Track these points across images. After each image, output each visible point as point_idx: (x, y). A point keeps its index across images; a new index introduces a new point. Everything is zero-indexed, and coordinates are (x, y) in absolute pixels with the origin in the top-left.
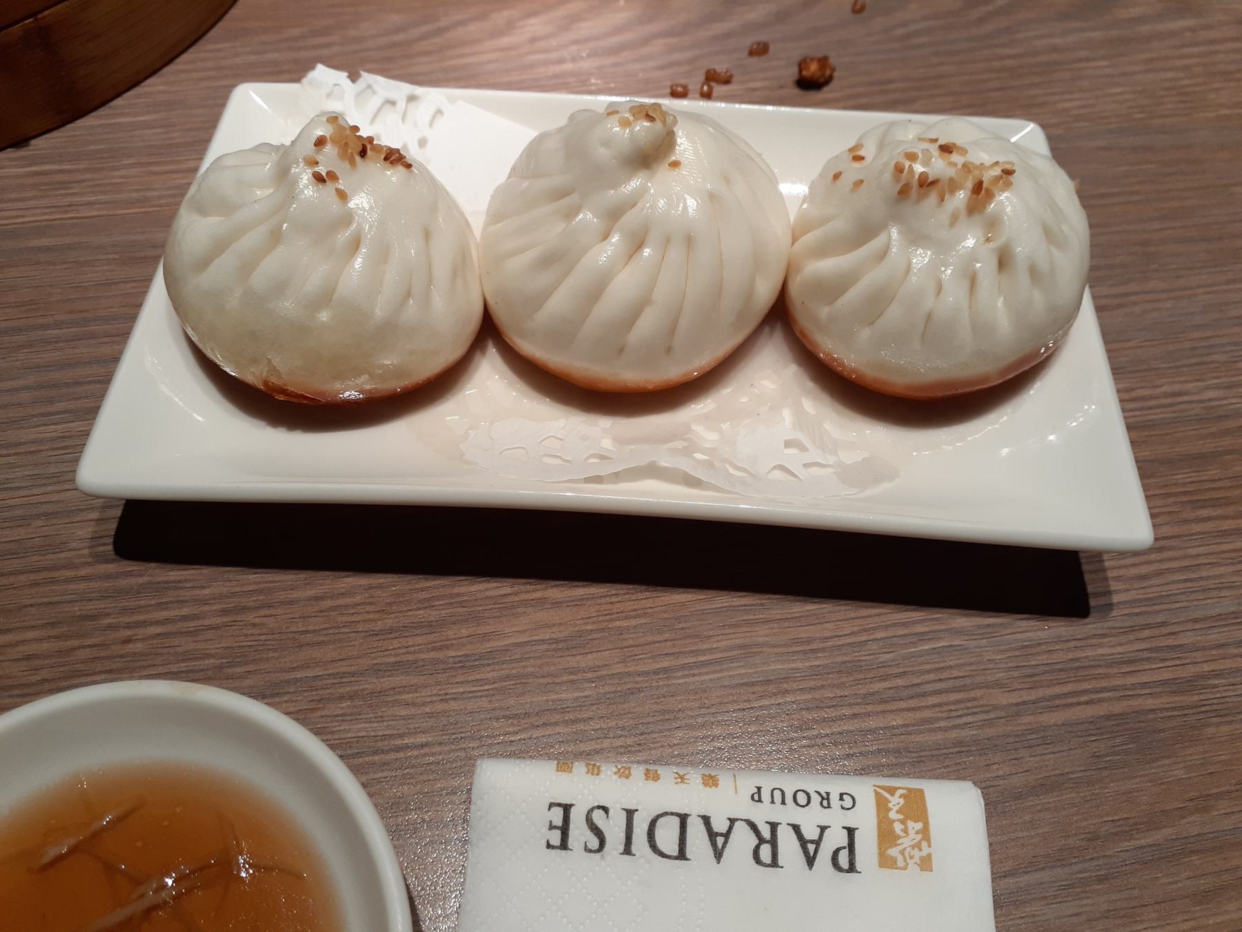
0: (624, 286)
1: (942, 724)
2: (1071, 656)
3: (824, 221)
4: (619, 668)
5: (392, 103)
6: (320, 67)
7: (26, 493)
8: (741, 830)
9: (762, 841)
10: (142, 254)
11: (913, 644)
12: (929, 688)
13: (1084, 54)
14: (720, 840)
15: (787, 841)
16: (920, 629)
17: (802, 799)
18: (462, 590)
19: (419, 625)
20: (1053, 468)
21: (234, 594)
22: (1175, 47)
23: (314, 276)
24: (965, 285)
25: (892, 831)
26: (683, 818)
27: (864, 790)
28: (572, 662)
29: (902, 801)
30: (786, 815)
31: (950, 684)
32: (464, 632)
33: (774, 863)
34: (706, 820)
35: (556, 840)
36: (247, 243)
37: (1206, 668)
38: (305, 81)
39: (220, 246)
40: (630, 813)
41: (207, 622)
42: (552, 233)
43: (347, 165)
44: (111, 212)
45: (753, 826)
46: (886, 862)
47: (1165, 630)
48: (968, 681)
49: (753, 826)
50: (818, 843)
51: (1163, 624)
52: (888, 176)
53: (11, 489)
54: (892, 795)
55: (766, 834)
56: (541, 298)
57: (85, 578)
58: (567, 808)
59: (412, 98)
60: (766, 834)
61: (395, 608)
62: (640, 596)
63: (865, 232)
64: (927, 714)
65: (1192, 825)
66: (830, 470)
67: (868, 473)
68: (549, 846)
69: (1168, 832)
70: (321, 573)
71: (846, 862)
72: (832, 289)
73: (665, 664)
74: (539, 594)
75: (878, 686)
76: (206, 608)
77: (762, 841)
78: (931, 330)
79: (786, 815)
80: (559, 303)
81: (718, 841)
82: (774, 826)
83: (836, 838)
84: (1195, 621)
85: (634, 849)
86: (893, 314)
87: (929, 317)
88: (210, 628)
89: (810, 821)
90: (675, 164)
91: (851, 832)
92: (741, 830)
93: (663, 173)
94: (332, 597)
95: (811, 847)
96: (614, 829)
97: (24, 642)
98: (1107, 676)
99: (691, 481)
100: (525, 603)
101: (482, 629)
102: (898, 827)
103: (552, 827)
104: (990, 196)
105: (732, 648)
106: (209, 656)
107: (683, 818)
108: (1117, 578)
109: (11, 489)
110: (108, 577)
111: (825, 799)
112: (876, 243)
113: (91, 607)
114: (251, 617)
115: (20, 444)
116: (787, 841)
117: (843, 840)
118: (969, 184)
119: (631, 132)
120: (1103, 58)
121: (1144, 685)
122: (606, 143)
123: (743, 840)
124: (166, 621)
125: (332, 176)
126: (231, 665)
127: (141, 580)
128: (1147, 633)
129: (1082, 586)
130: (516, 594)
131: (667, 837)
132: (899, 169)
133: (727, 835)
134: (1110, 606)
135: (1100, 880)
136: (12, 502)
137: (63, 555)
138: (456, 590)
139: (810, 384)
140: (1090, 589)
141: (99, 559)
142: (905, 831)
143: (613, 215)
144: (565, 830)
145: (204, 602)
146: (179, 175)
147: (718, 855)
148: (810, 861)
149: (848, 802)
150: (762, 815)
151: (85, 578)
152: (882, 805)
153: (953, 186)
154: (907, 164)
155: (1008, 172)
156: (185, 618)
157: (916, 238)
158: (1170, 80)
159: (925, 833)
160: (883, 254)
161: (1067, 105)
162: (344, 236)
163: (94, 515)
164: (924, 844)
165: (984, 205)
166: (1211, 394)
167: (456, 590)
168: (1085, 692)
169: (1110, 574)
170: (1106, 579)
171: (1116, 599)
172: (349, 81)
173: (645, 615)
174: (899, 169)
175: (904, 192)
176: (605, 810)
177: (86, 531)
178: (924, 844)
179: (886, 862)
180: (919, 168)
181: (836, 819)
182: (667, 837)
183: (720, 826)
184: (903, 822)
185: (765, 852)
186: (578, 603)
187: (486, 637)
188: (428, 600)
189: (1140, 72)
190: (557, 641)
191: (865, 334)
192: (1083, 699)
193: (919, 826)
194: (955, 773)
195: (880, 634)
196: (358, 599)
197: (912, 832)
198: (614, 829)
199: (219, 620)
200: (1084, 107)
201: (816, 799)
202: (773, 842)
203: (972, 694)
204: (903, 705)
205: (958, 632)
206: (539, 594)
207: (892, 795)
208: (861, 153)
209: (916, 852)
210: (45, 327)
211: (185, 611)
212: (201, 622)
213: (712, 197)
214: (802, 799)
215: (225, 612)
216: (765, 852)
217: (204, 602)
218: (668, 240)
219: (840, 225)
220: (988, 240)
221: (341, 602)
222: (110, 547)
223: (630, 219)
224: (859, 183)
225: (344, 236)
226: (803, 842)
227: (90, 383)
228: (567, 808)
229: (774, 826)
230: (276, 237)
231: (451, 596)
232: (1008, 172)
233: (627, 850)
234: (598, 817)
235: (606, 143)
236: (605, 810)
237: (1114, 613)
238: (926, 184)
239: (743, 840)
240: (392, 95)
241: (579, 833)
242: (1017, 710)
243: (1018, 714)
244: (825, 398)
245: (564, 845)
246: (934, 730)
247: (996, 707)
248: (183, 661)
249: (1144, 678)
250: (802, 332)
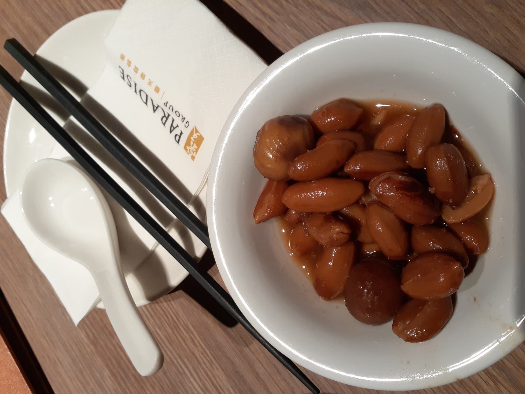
25: (190, 143)
29: (197, 137)
50: (174, 128)
54: (196, 133)
55: (167, 115)
60: (167, 115)
77: (165, 116)
82: (169, 115)
83: (177, 131)
89: (178, 121)
91: (181, 133)
95: (172, 128)
102: (192, 143)
111: (184, 119)
116: (170, 121)
117: (179, 134)
142: (193, 145)
150: (167, 110)
159: (197, 150)
164: (195, 153)
178: (195, 153)
181: (182, 126)
184: (193, 142)
185: (164, 119)
193: (196, 147)
197: (194, 147)
201: (181, 117)
202: (167, 119)
207: (196, 133)
216: (164, 119)
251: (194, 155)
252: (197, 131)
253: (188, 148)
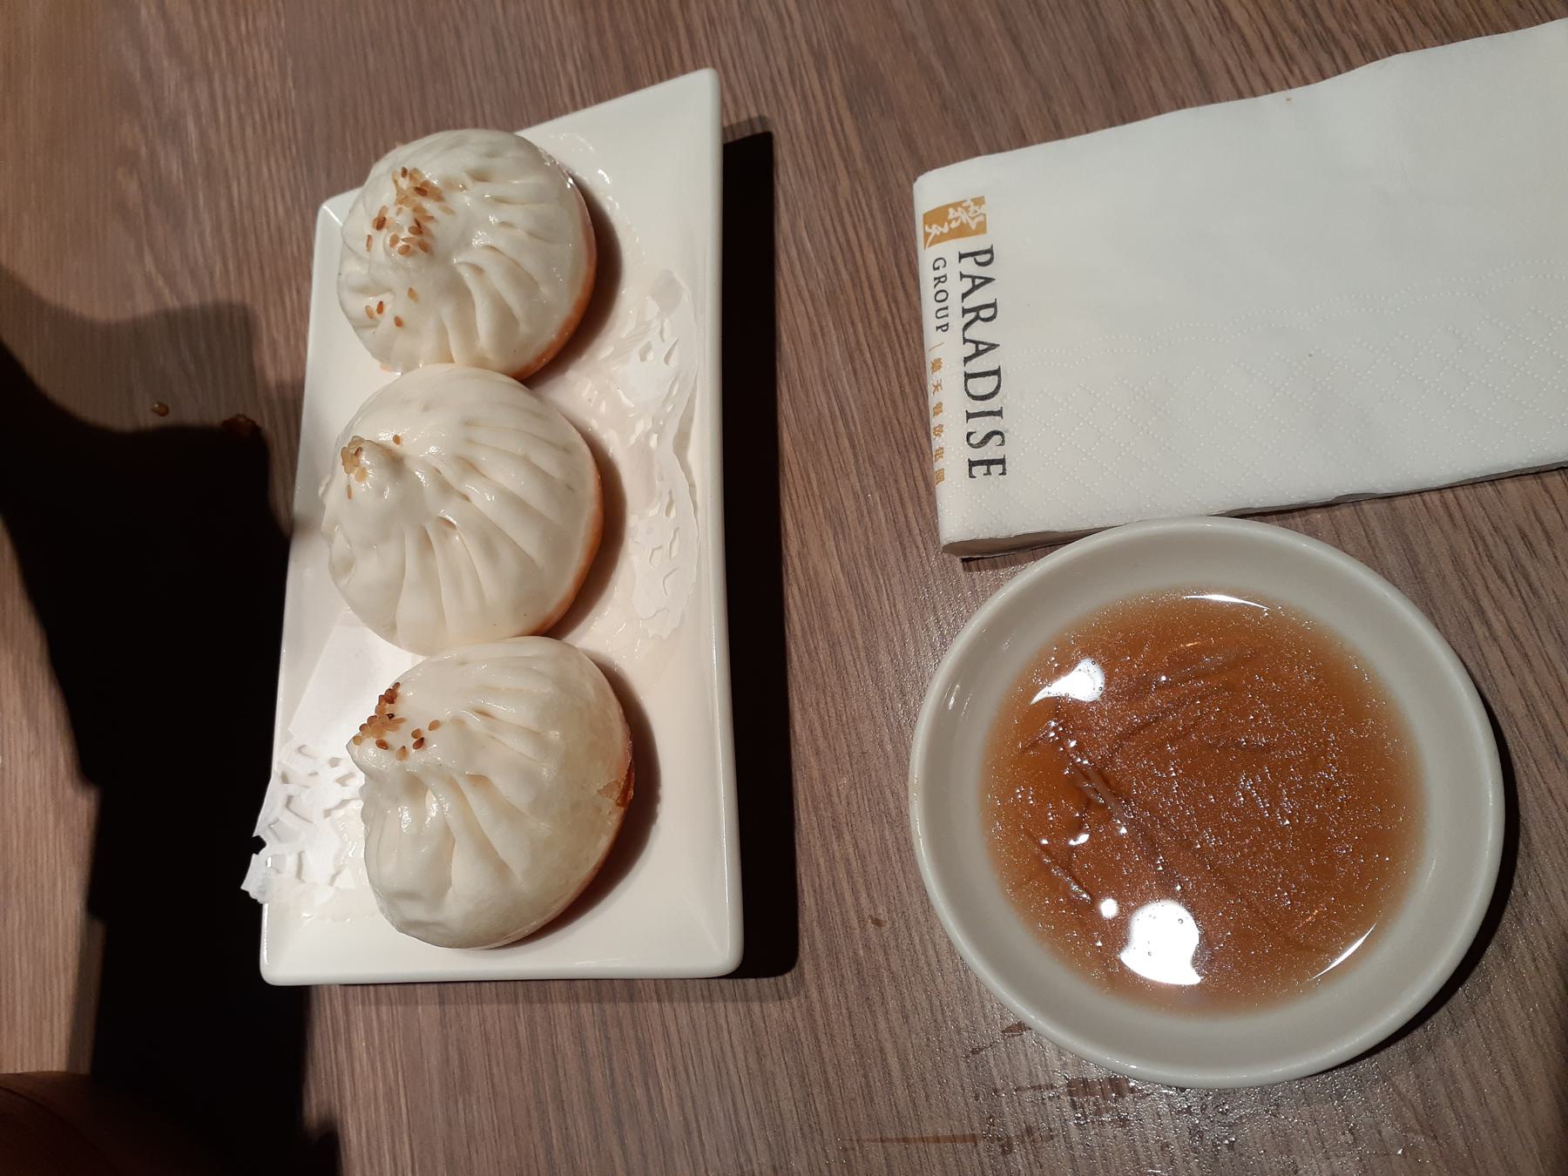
0: (510, 477)
1: (870, 223)
2: (805, 141)
3: (442, 332)
4: (854, 478)
5: (290, 799)
6: (243, 887)
7: (738, 1091)
8: (972, 333)
9: (977, 318)
10: (457, 1071)
11: (808, 258)
12: (842, 239)
13: (223, 204)
14: (981, 347)
16: (794, 253)
17: (942, 296)
18: (798, 627)
19: (833, 653)
20: (652, 160)
21: (821, 832)
22: (218, 130)
23: (518, 747)
24: (505, 206)
26: (968, 376)
27: (927, 256)
28: (852, 517)
30: (955, 304)
31: (837, 224)
32: (836, 614)
33: (994, 305)
34: (967, 360)
35: (999, 468)
36: (481, 811)
37: (804, 47)
38: (260, 900)
39: (485, 849)
40: (969, 416)
41: (851, 850)
42: (463, 545)
43: (403, 726)
44: (405, 1128)
46: (981, 229)
47: (777, 79)
48: (834, 211)
50: (973, 278)
51: (772, 80)
52: (410, 263)
53: (735, 1110)
55: (972, 316)
56: (524, 560)
57: (821, 989)
58: (972, 464)
59: (285, 779)
60: (972, 316)
61: (820, 681)
62: (789, 476)
63: (457, 291)
64: (863, 235)
65: (926, 45)
66: (667, 323)
67: (667, 291)
68: (1004, 473)
69: (934, 59)
70: (794, 757)
71: (986, 256)
72: (505, 319)
73: (846, 443)
74: (796, 560)
75: (845, 277)
76: (837, 854)
77: (977, 318)
78: (542, 234)
79: (955, 304)
80: (528, 540)
81: (982, 349)
82: (965, 311)
83: (969, 266)
84: (767, 58)
85: (996, 409)
86: (530, 264)
87: (531, 234)
88: (856, 845)
89: (956, 287)
90: (397, 439)
91: (962, 256)
92: (972, 333)
93: (404, 449)
94: (815, 741)
95: (978, 282)
96: (983, 426)
97: (891, 1030)
98: (819, 114)
99: (686, 421)
100: (805, 570)
101: (832, 600)
102: (954, 225)
103: (989, 473)
104: (426, 183)
105: (827, 392)
106: (883, 837)
107: (968, 376)
108: (737, 116)
109: (735, 1110)
110: (817, 966)
111: (938, 280)
112: (467, 276)
113: (849, 974)
114: (841, 809)
115: (685, 1119)
116: (975, 300)
117: (971, 259)
118: (418, 199)
119: (371, 467)
120: (229, 188)
121: (823, 87)
122: (380, 492)
123: (979, 331)
124: (854, 891)
125: (416, 734)
126: (888, 814)
127: (817, 931)
128: (781, 90)
129: (745, 140)
130: (797, 580)
131: (983, 386)
132: (406, 251)
133: (977, 343)
134: (762, 119)
135: (974, 97)
136: (749, 1102)
137: (800, 1025)
138: (799, 633)
139: (584, 358)
140: (748, 134)
141: (800, 981)
143: (445, 488)
144: (989, 463)
145: (831, 860)
146: (357, 1065)
147: (993, 346)
148: (988, 280)
149: (940, 263)
151: (821, 989)
152: (939, 239)
153: (418, 209)
154: (401, 244)
155: (404, 172)
156: (849, 873)
157: (464, 242)
158: (254, 129)
159: (956, 206)
160: (478, 270)
161: (281, 209)
162: (475, 723)
163: (756, 1007)
165: (434, 188)
166: (570, 68)
167: (799, 633)
168: (833, 128)
169: (734, 121)
170: (739, 124)
171: (754, 114)
172: (263, 851)
173: (806, 469)
174: (406, 251)
175: (425, 248)
176: (969, 434)
177: (773, 1008)
179: (981, 229)
180: (405, 234)
181: (953, 269)
182: (983, 386)
183: (970, 349)
184: (950, 222)
185: (984, 314)
186: (800, 526)
187: (839, 596)
188: (810, 655)
189: (246, 157)
190: (835, 534)
191: (545, 290)
192: (838, 126)
193: (951, 210)
194: (908, 202)
195: (802, 282)
196: (815, 717)
198: (983, 426)
199: (847, 837)
200: (283, 196)
201: (940, 286)
203: (843, 206)
204: (858, 255)
205: (793, 225)
206: (796, 560)
208: (375, 307)
209: (973, 208)
210: (549, 1149)
211: (842, 875)
212: (852, 856)
213: (426, 408)
214: (941, 296)
215: (839, 836)
216: (984, 314)
217: (831, 860)
218: (470, 441)
219: (447, 311)
220: (464, 188)
221: (819, 732)
222: (787, 976)
223: (449, 474)
224: (412, 293)
225: (475, 723)
226: (975, 288)
227: (612, 1070)
228: (972, 464)
229: (965, 311)
230: (479, 780)
231: (804, 635)
232: (404, 172)
233: (999, 413)
234: (974, 440)
235: (380, 492)
236: (969, 434)
237: (766, 114)
238: (418, 229)
239: (979, 331)
240: (281, 800)
242: (853, 173)
243: (856, 172)
244: (597, 342)
245: (1002, 462)
246: (876, 229)
247: (853, 189)
248: (889, 858)
249: (817, 87)
250: (539, 359)
251: (969, 203)
253: (973, 225)
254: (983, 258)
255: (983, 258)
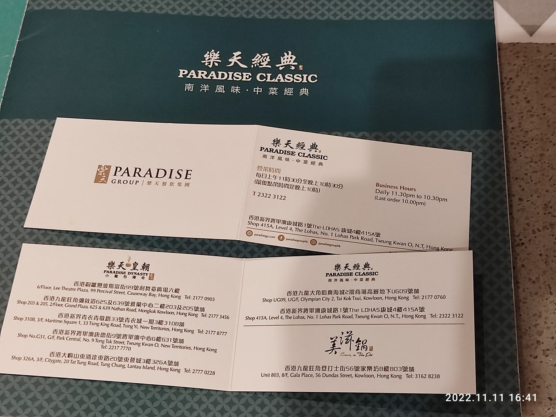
15: (132, 173)
30: (131, 178)
40: (170, 177)
45: (140, 176)
46: (109, 167)
49: (140, 176)
55: (137, 174)
58: (186, 178)
60: (137, 174)
107: (157, 177)
131: (161, 173)
142: (102, 173)
144: (187, 174)
152: (106, 179)
159: (98, 172)
185: (138, 170)
241: (184, 174)
252: (103, 182)
254: (119, 169)
255: (119, 169)
